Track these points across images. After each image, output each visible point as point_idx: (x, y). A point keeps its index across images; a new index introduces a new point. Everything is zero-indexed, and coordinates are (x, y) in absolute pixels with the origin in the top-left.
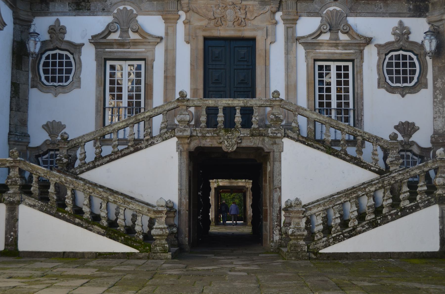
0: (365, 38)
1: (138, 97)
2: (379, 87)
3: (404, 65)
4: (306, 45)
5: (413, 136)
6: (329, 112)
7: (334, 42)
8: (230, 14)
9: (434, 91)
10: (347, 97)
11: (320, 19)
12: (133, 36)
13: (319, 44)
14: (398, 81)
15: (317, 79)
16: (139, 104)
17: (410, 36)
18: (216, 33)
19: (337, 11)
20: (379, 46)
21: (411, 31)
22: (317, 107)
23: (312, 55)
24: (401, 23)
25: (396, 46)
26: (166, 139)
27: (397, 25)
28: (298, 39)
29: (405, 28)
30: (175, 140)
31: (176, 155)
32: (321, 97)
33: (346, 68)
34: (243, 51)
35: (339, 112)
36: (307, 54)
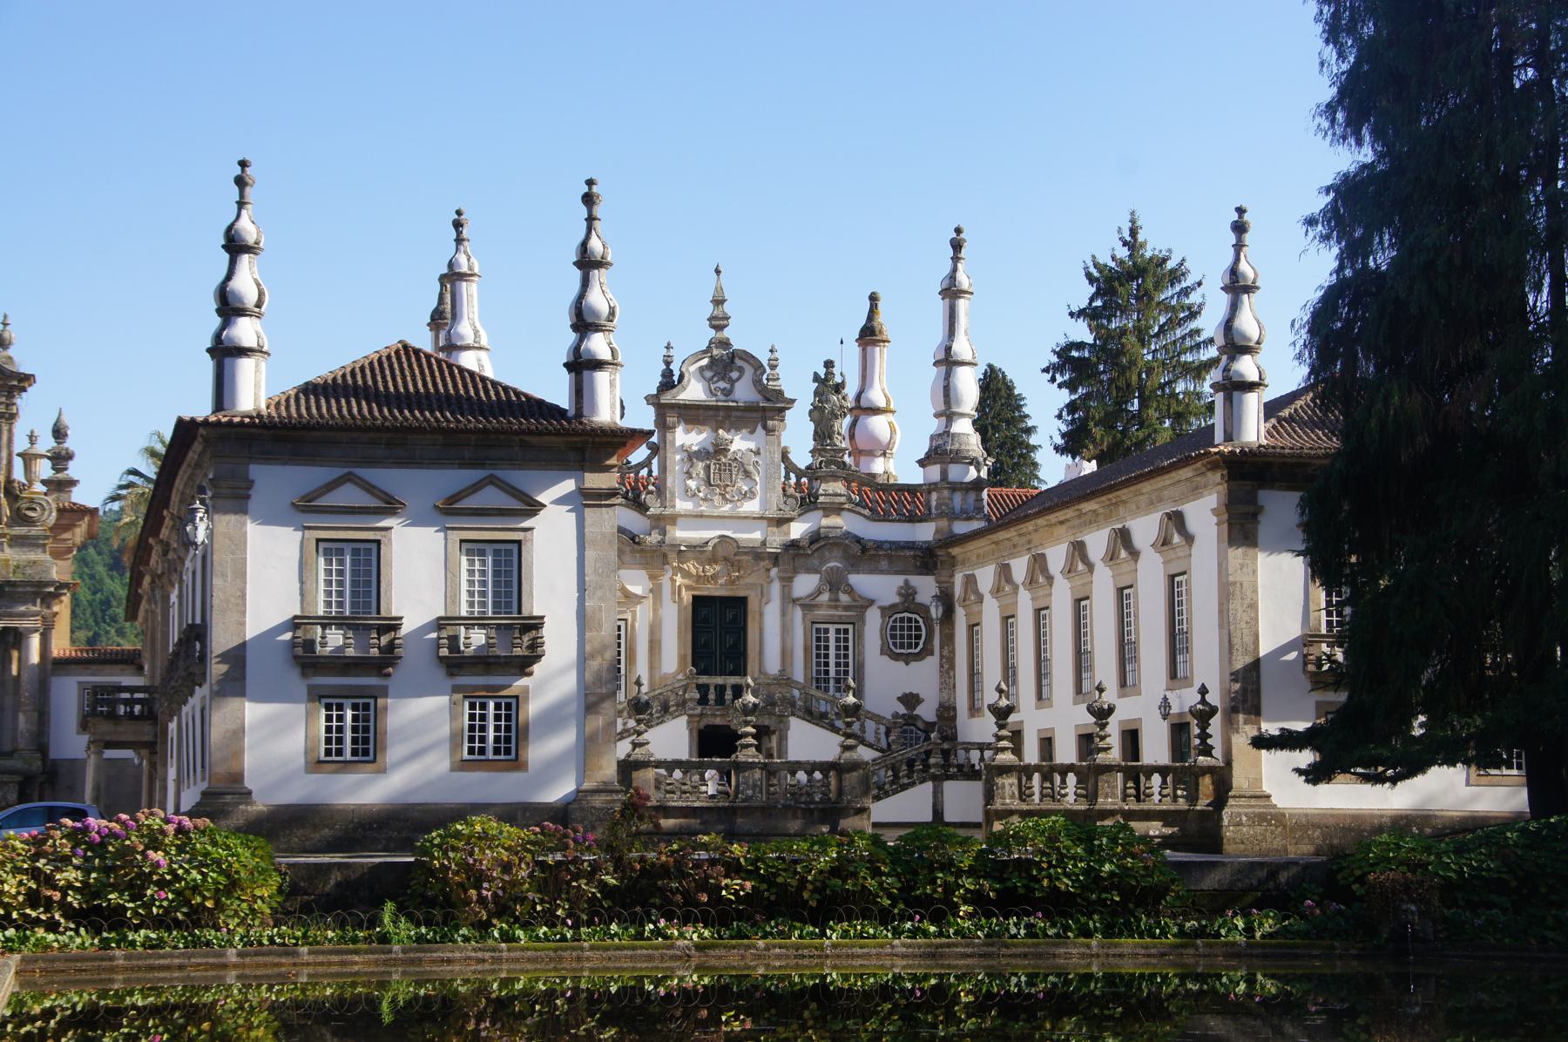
0: (868, 600)
2: (882, 653)
4: (803, 606)
5: (918, 708)
6: (827, 681)
7: (833, 604)
9: (941, 660)
10: (847, 665)
11: (817, 577)
13: (816, 606)
14: (902, 646)
15: (814, 643)
17: (916, 596)
19: (838, 568)
20: (882, 609)
21: (918, 590)
22: (814, 675)
24: (906, 582)
25: (901, 607)
26: (677, 717)
27: (902, 584)
28: (794, 601)
29: (911, 587)
30: (685, 718)
31: (686, 734)
32: (818, 664)
33: (846, 631)
36: (804, 616)
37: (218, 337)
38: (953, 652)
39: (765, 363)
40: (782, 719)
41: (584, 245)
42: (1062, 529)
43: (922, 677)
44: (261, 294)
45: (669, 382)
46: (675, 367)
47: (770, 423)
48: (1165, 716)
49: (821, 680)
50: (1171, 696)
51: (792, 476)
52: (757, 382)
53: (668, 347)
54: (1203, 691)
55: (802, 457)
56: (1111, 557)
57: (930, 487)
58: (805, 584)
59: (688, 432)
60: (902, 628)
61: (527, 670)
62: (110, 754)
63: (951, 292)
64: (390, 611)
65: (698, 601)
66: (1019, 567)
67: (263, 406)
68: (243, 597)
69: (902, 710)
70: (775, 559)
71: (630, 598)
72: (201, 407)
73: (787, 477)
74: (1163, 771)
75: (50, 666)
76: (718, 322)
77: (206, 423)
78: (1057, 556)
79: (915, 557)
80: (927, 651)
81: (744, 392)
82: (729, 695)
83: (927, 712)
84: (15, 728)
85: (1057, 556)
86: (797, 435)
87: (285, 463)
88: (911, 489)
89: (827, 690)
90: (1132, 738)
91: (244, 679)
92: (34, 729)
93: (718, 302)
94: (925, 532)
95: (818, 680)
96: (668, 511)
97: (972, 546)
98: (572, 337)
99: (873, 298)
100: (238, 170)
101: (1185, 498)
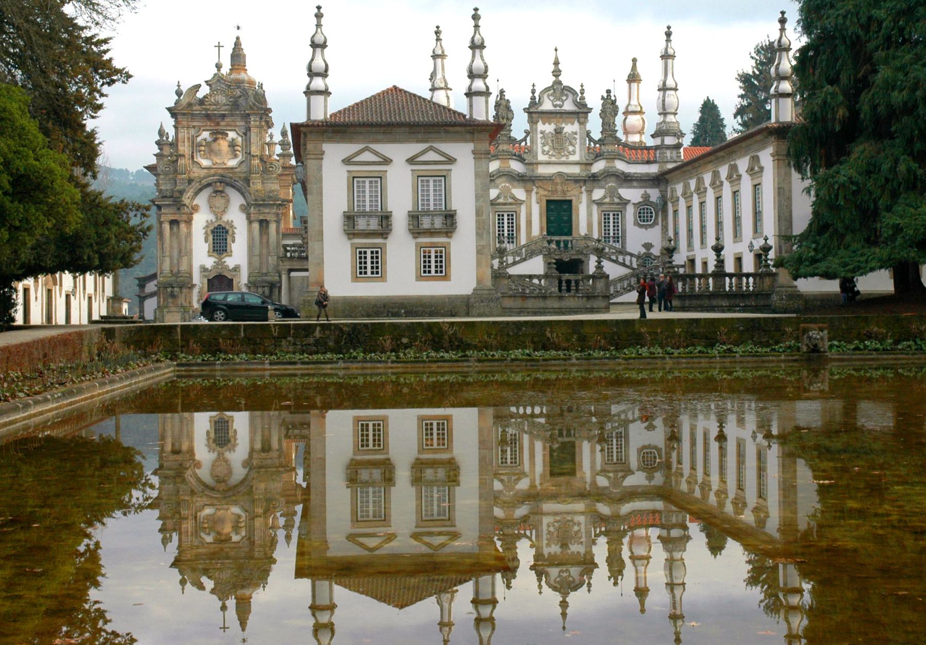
1: (513, 231)
3: (647, 213)
6: (609, 238)
8: (559, 188)
10: (618, 230)
12: (510, 200)
14: (644, 221)
16: (513, 234)
18: (552, 198)
20: (634, 204)
23: (601, 209)
24: (645, 192)
28: (594, 201)
32: (605, 230)
33: (618, 215)
34: (565, 207)
35: (614, 237)
37: (308, 87)
38: (667, 223)
39: (578, 92)
40: (587, 256)
41: (473, 38)
42: (710, 166)
43: (654, 236)
44: (327, 66)
45: (533, 103)
46: (537, 95)
47: (582, 120)
48: (751, 251)
49: (607, 238)
50: (754, 242)
51: (592, 144)
52: (575, 102)
53: (533, 85)
54: (766, 239)
55: (596, 135)
56: (729, 177)
57: (657, 148)
58: (598, 194)
59: (544, 124)
60: (644, 213)
61: (449, 234)
62: (293, 274)
63: (667, 56)
64: (387, 209)
65: (549, 202)
66: (693, 183)
67: (328, 117)
68: (321, 203)
69: (643, 250)
70: (585, 181)
71: (518, 203)
72: (301, 119)
73: (589, 144)
74: (748, 276)
75: (281, 236)
76: (557, 73)
77: (302, 125)
78: (707, 178)
79: (649, 180)
80: (655, 223)
81: (568, 106)
82: (562, 245)
83: (656, 251)
84: (268, 263)
85: (707, 178)
86: (595, 125)
87: (338, 142)
88: (648, 149)
89: (609, 241)
90: (739, 260)
91: (322, 240)
92: (275, 263)
93: (556, 63)
94: (653, 169)
95: (605, 238)
96: (534, 161)
97: (673, 174)
98: (468, 81)
99: (634, 60)
100: (316, 11)
101: (759, 150)
